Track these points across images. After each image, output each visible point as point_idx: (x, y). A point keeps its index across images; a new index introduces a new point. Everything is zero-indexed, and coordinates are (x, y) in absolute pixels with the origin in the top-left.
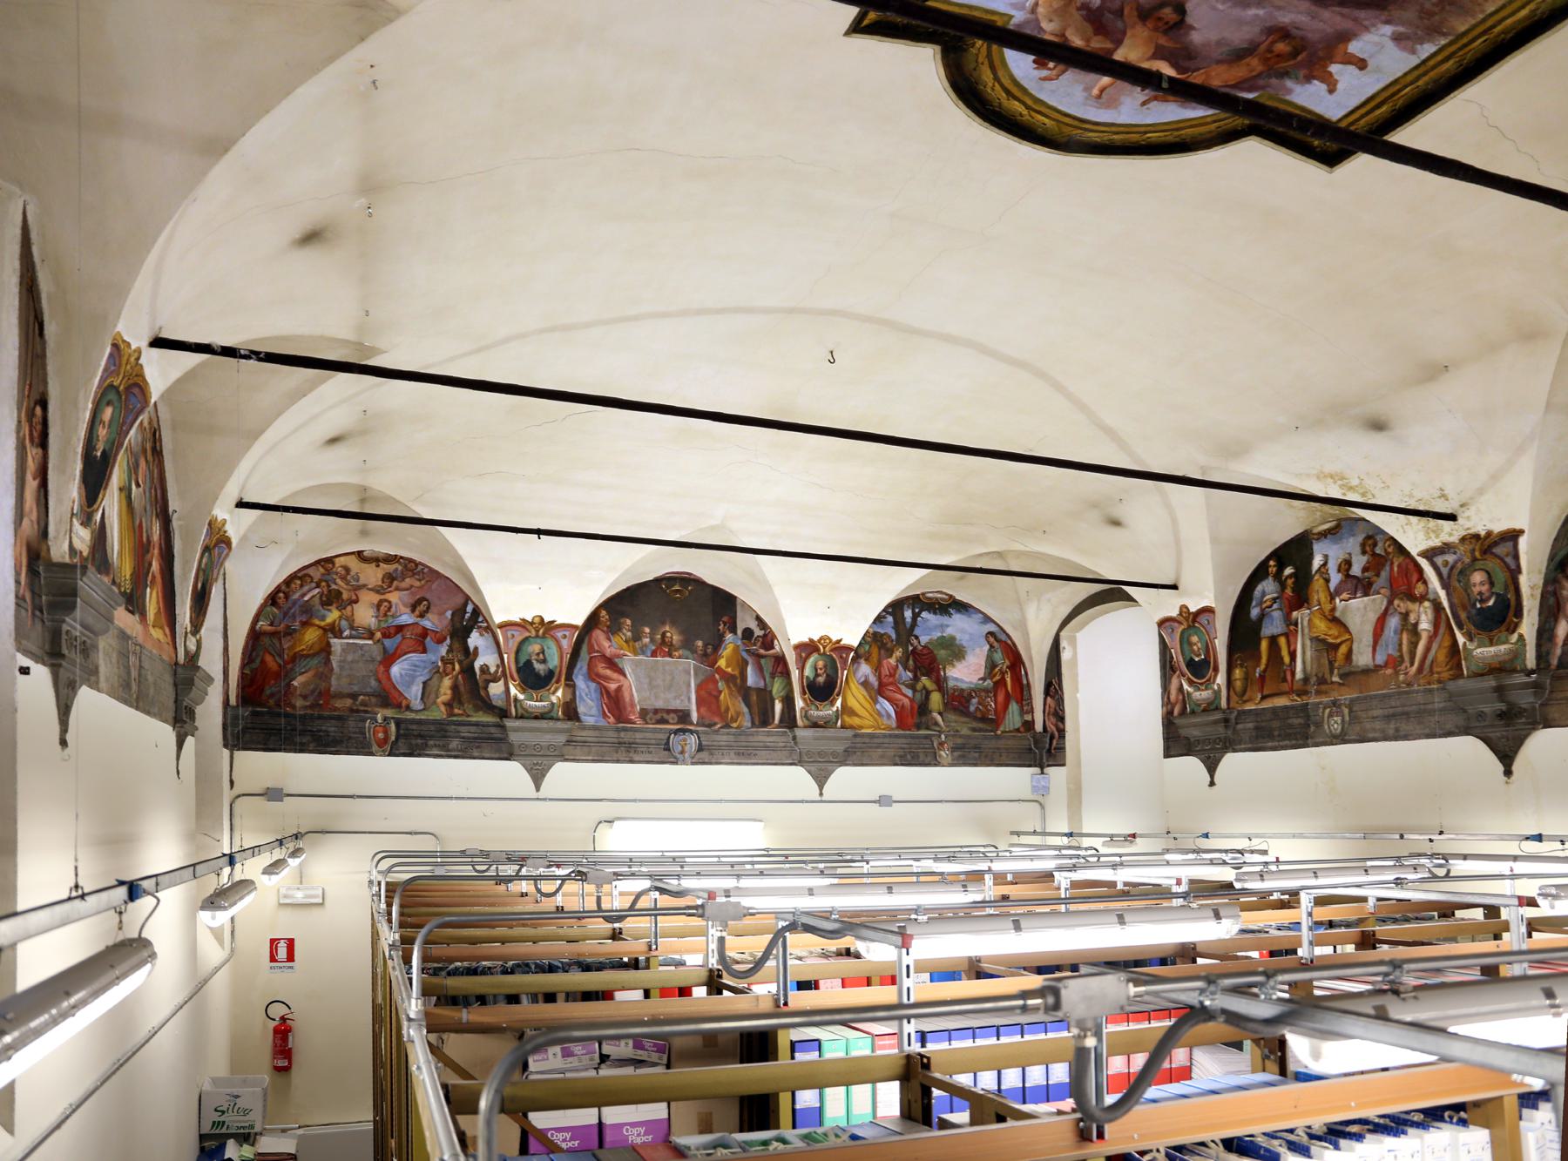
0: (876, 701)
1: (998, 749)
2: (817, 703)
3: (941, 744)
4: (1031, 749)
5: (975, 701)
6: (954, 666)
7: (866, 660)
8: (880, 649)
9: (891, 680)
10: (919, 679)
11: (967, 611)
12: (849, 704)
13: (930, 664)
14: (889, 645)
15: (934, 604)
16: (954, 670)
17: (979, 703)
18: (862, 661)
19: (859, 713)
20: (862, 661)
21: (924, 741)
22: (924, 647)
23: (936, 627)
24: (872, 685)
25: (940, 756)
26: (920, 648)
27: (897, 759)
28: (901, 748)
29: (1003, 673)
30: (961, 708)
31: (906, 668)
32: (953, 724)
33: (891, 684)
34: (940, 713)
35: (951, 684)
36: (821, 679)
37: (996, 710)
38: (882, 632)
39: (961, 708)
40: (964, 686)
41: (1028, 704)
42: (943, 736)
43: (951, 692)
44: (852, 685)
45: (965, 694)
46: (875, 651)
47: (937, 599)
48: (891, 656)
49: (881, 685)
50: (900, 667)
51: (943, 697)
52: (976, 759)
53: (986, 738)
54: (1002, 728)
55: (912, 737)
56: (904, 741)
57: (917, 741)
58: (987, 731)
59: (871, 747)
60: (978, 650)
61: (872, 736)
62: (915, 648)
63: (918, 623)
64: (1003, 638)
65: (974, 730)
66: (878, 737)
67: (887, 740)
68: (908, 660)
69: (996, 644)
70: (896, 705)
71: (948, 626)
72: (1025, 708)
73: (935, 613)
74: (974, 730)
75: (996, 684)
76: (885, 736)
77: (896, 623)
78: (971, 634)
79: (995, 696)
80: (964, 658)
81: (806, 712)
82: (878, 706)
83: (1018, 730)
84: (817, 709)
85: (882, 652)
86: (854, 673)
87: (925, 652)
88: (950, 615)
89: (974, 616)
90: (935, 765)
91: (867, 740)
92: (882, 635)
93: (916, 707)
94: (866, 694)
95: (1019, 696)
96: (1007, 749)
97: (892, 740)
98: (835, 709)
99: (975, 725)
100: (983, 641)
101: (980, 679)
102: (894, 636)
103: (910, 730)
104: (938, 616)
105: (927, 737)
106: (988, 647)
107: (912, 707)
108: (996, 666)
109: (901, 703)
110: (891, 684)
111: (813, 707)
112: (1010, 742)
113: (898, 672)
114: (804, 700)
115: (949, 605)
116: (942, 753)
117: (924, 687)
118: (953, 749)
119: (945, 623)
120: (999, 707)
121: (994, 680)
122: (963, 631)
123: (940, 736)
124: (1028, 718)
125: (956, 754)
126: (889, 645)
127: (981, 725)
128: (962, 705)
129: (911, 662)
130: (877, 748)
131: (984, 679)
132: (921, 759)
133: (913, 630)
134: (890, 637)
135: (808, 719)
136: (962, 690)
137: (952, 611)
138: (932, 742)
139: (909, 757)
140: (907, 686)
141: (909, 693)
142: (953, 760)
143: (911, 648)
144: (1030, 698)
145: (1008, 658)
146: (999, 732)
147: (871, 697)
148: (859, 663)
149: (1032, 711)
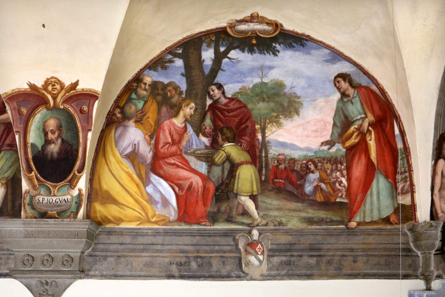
0: (146, 182)
1: (352, 250)
2: (49, 184)
3: (252, 244)
4: (410, 250)
5: (313, 177)
6: (279, 125)
7: (136, 122)
8: (160, 105)
9: (174, 149)
10: (221, 146)
11: (303, 45)
12: (105, 187)
13: (240, 123)
14: (175, 99)
15: (250, 38)
16: (280, 131)
17: (321, 180)
18: (131, 123)
19: (121, 200)
20: (131, 123)
21: (223, 240)
22: (231, 99)
23: (252, 70)
24: (143, 159)
25: (248, 263)
26: (224, 101)
27: (174, 269)
28: (182, 251)
29: (363, 135)
30: (290, 188)
31: (199, 130)
32: (272, 213)
33: (172, 155)
34: (253, 197)
35: (273, 152)
36: (54, 148)
37: (348, 189)
38: (166, 81)
39: (290, 188)
40: (296, 155)
41: (404, 180)
42: (255, 233)
43: (272, 164)
44: (111, 158)
45: (297, 167)
46: (152, 108)
47: (254, 32)
48: (176, 115)
49: (157, 156)
50: (190, 130)
51: (260, 171)
52: (310, 267)
53: (330, 234)
54: (358, 218)
55: (201, 234)
56: (187, 240)
57: (210, 240)
58: (332, 222)
59: (133, 250)
60: (321, 102)
61: (135, 233)
62: (216, 102)
63: (223, 66)
64: (364, 81)
65: (310, 221)
66: (147, 235)
67: (159, 239)
68: (203, 119)
69: (351, 91)
70: (180, 187)
71: (271, 68)
72: (400, 186)
73: (251, 51)
74: (310, 221)
75: (351, 150)
76: (156, 233)
77: (187, 66)
78: (309, 78)
79: (349, 169)
80: (297, 113)
81: (32, 198)
82: (150, 189)
83: (387, 220)
84: (49, 193)
85: (164, 109)
86: (116, 143)
87: (232, 106)
88: (275, 52)
89: (313, 52)
90: (239, 278)
91: (127, 239)
92: (165, 87)
93: (212, 187)
94: (131, 170)
95: (390, 168)
96: (364, 250)
97: (168, 239)
98: (75, 192)
99: (312, 213)
100: (330, 87)
101: (322, 144)
102: (184, 87)
103: (199, 224)
104: (257, 55)
105: (226, 234)
106: (337, 96)
107: (205, 187)
108: (352, 123)
109: (186, 184)
110: (172, 155)
111: (43, 191)
112: (371, 239)
113: (186, 138)
114: (30, 180)
115: (275, 39)
116: (252, 259)
117: (228, 158)
118: (272, 253)
119: (268, 63)
120: (355, 184)
121: (348, 144)
122: (296, 74)
123: (250, 233)
124: (405, 200)
125: (276, 260)
126: (175, 99)
127: (322, 214)
128: (291, 183)
129: (208, 122)
130: (143, 250)
131: (330, 143)
132: (215, 268)
133: (215, 77)
134: (176, 88)
135: (33, 208)
136: (293, 161)
137: (278, 47)
138: (234, 240)
139: (194, 265)
140: (199, 157)
141: (202, 167)
142: (270, 269)
143: (209, 102)
144: (410, 169)
145: (373, 112)
146: (353, 224)
147: (139, 176)
148: (126, 127)
149: (412, 190)
